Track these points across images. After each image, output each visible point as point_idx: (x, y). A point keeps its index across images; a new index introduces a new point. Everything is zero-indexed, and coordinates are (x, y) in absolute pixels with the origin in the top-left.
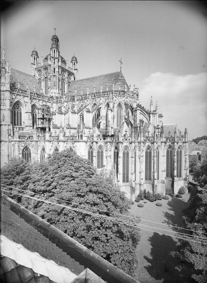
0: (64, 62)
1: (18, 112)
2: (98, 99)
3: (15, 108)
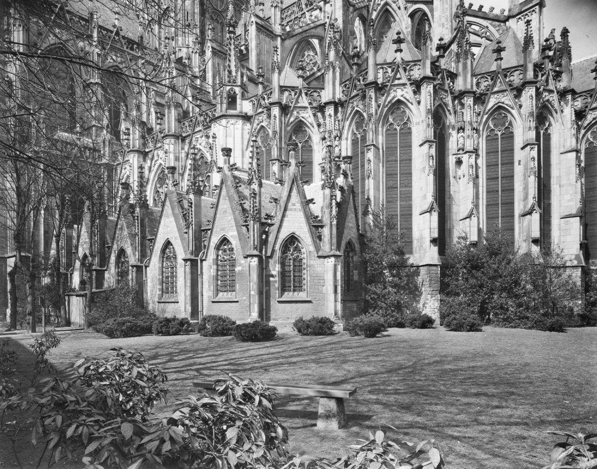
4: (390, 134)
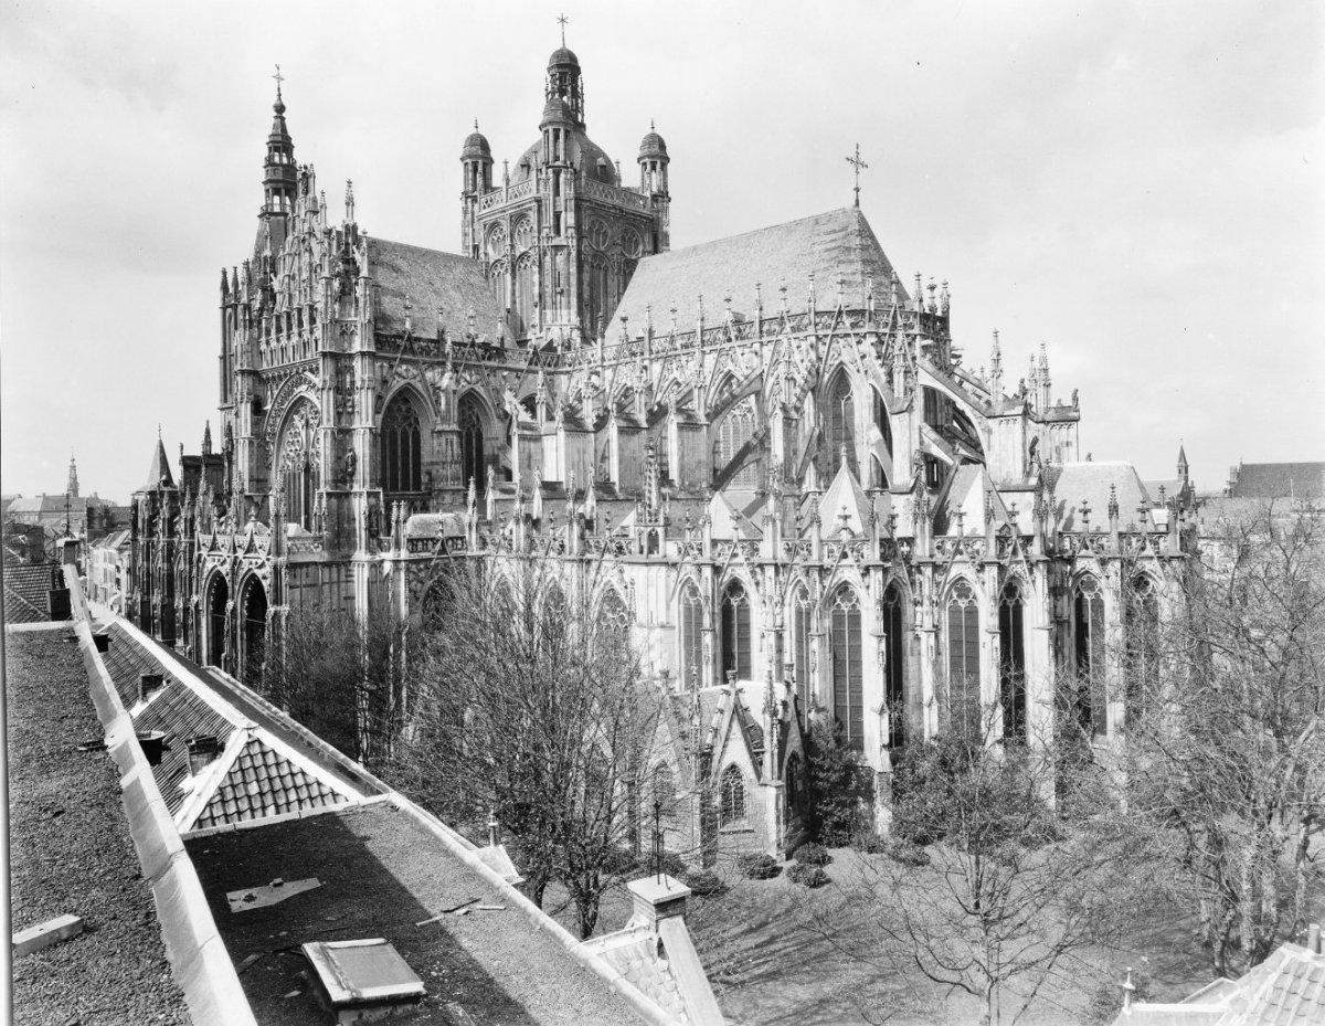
0: (604, 173)
1: (405, 434)
2: (746, 350)
3: (394, 419)
4: (838, 619)
